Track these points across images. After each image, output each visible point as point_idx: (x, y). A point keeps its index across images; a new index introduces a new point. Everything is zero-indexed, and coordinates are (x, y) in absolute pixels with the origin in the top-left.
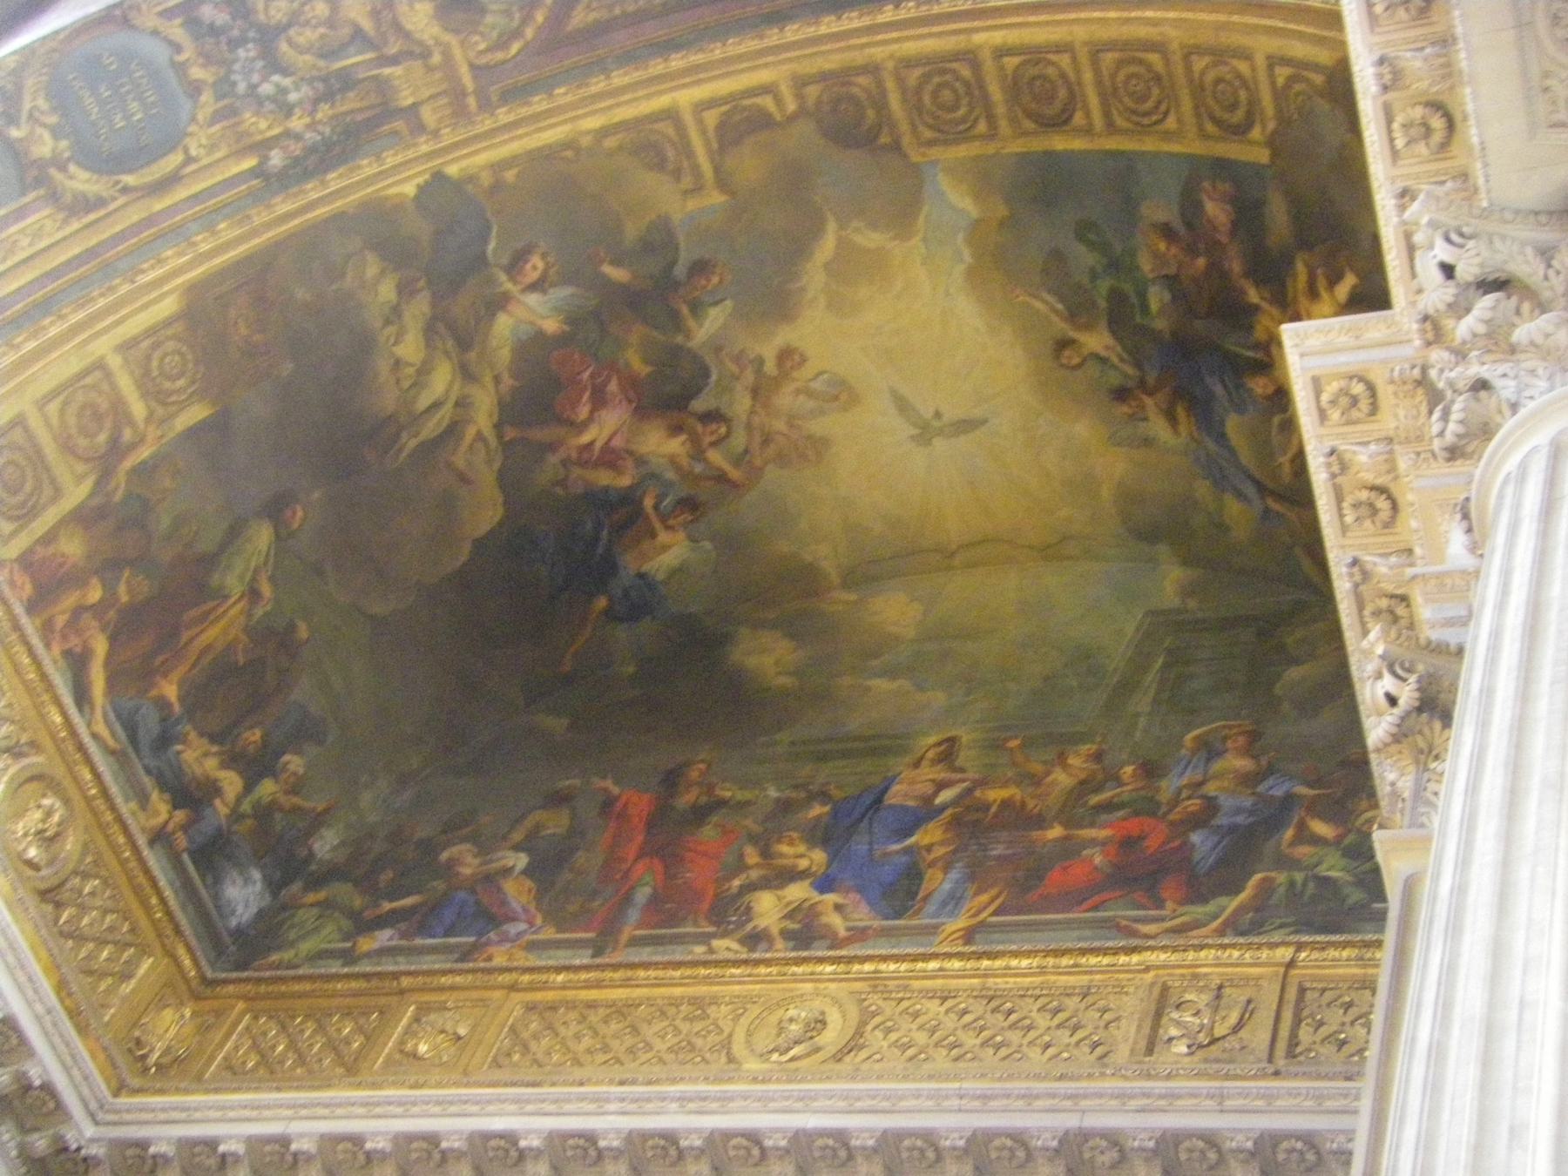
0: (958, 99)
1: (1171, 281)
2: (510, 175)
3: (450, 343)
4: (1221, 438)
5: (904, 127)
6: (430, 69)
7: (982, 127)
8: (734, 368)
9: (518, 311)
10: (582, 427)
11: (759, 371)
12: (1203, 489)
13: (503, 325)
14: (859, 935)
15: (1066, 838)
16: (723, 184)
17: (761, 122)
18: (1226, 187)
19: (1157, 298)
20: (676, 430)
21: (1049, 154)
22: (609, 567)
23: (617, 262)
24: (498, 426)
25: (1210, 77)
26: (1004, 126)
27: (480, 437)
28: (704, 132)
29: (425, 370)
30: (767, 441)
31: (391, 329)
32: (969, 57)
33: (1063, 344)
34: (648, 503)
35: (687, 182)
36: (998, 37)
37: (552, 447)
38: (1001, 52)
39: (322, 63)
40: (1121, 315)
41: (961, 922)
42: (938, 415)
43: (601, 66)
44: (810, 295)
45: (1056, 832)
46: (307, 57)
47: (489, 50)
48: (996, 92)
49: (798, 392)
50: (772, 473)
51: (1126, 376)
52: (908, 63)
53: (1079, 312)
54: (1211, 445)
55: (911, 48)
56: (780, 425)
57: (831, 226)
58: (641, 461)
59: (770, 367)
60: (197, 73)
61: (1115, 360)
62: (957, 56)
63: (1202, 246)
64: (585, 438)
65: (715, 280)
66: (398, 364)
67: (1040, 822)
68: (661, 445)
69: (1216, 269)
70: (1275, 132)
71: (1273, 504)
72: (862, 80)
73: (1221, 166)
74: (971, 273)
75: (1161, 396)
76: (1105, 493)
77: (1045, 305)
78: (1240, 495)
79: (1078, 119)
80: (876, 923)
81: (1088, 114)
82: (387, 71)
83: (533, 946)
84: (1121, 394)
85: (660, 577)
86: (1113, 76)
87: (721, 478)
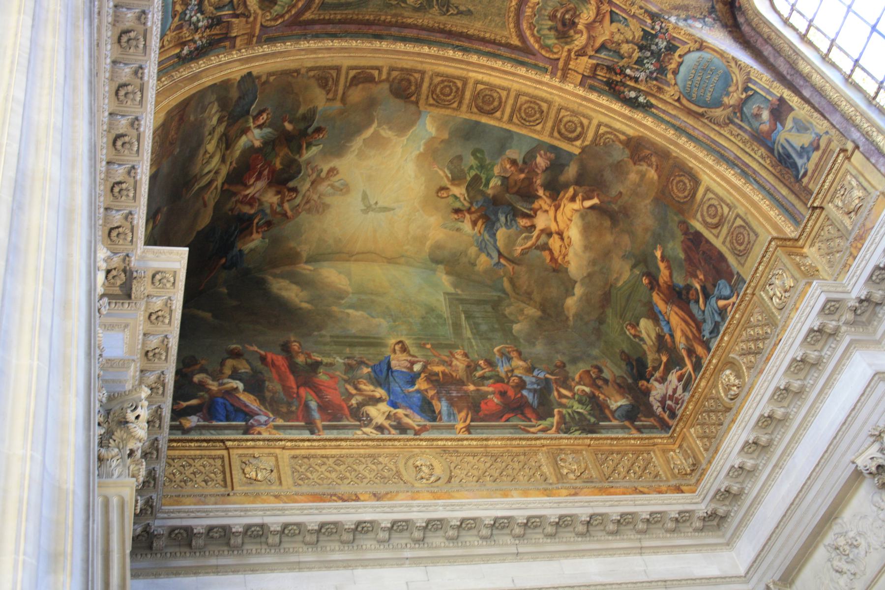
0: (451, 92)
1: (505, 179)
2: (272, 79)
3: (224, 145)
4: (493, 236)
5: (423, 97)
6: (247, 22)
7: (455, 105)
8: (310, 171)
9: (250, 135)
10: (247, 187)
11: (319, 175)
12: (473, 250)
13: (243, 141)
14: (424, 429)
15: (478, 390)
16: (343, 100)
17: (370, 79)
18: (553, 156)
19: (495, 182)
20: (278, 193)
21: (478, 123)
22: (232, 246)
23: (290, 122)
24: (223, 184)
25: (565, 120)
26: (464, 107)
27: (216, 188)
28: (346, 78)
29: (211, 157)
30: (308, 202)
31: (210, 137)
32: (465, 81)
33: (443, 188)
34: (256, 221)
35: (331, 96)
36: (480, 77)
37: (235, 194)
38: (477, 82)
39: (214, 12)
40: (474, 185)
41: (460, 425)
42: (376, 203)
43: (305, 37)
44: (352, 149)
46: (212, 8)
47: (270, 20)
48: (468, 95)
49: (329, 185)
50: (303, 215)
51: (463, 205)
52: (438, 74)
53: (456, 179)
54: (487, 236)
55: (442, 69)
56: (315, 197)
57: (375, 125)
58: (261, 204)
59: (323, 175)
60: (178, 8)
61: (462, 199)
62: (458, 78)
63: (526, 171)
64: (248, 192)
65: (321, 136)
66: (206, 151)
68: (271, 198)
69: (529, 181)
70: (587, 146)
71: (502, 261)
72: (417, 75)
73: (553, 148)
74: (421, 154)
75: (474, 216)
76: (428, 243)
77: (443, 175)
78: (489, 255)
79: (498, 114)
80: (428, 423)
81: (503, 114)
82: (233, 20)
83: (277, 428)
84: (457, 211)
85: (246, 252)
86: (521, 105)
87: (285, 215)
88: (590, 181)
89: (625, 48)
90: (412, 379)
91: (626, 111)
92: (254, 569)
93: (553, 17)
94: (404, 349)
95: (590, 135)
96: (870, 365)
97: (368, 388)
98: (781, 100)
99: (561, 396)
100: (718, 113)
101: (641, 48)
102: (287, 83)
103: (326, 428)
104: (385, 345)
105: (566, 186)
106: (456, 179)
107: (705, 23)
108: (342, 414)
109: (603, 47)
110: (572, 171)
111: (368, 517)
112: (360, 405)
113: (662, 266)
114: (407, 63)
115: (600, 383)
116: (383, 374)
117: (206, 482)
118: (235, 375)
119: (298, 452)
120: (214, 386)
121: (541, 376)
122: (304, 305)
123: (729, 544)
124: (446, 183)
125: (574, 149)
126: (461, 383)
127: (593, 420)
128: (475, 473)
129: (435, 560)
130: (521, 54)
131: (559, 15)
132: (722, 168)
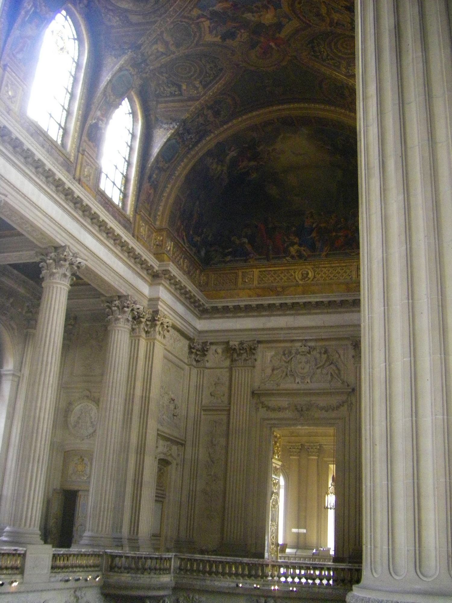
41: (324, 253)
45: (334, 234)
80: (311, 254)
94: (312, 216)
97: (292, 238)
103: (273, 258)
111: (272, 302)
119: (261, 270)
120: (237, 242)
128: (324, 275)
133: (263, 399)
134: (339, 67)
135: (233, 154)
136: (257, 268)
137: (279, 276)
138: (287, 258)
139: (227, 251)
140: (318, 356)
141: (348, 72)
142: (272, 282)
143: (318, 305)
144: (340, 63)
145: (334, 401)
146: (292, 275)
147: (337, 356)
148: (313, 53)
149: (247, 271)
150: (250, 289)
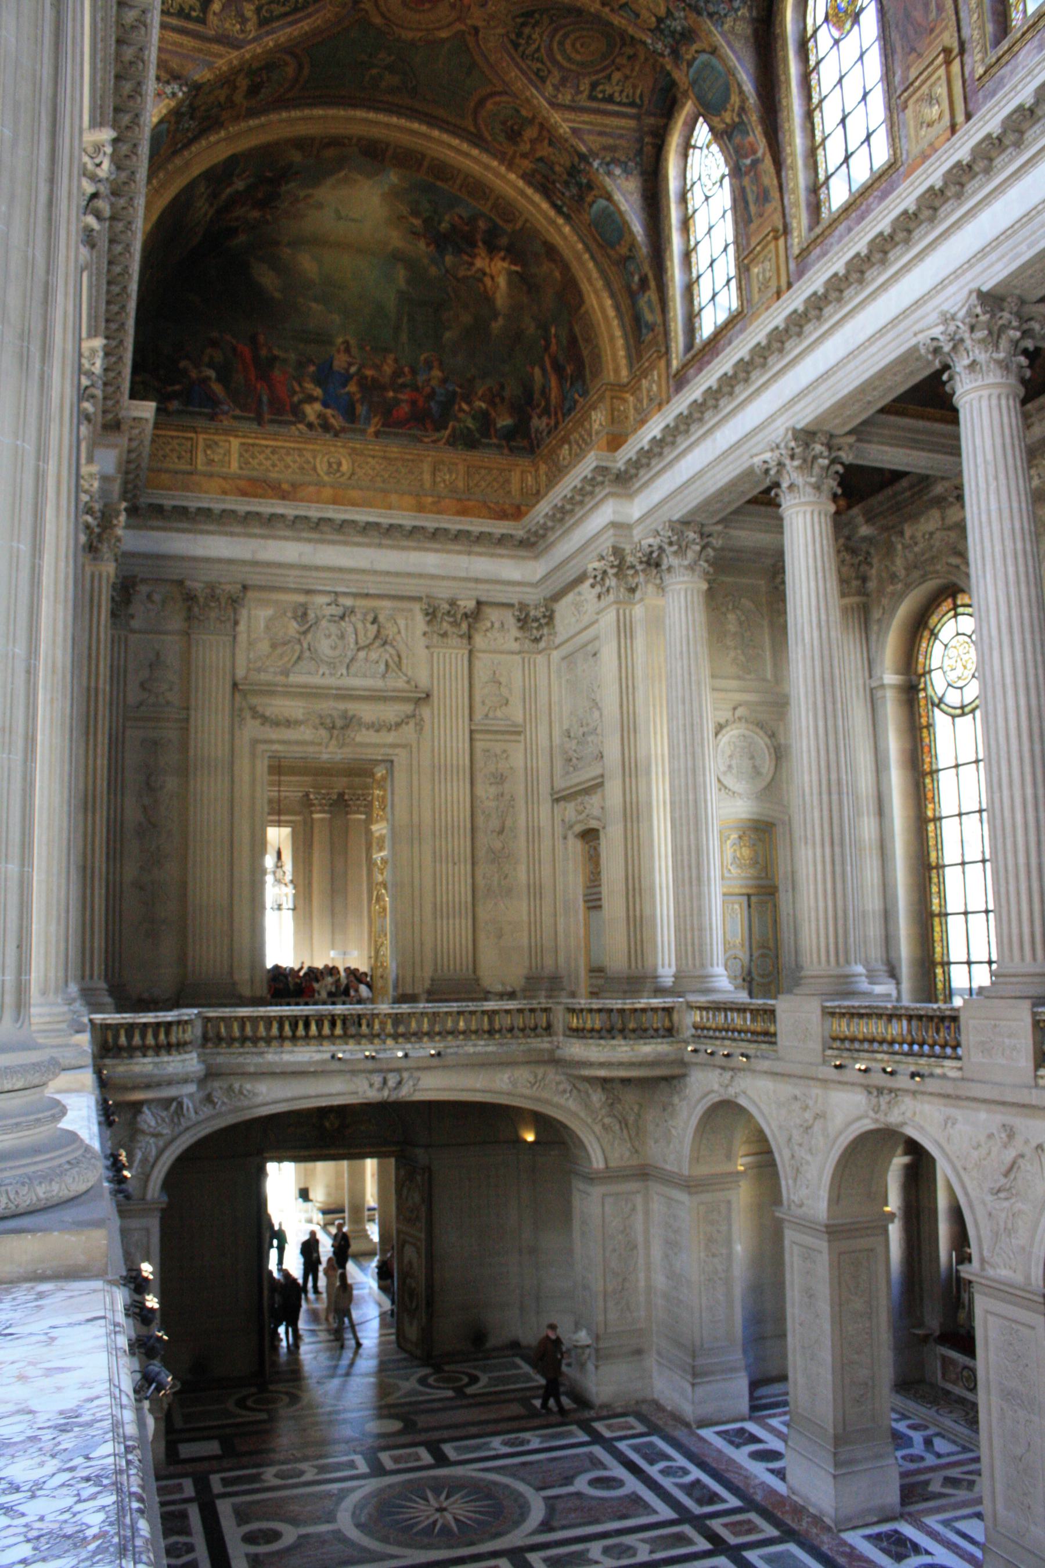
14: (343, 430)
33: (403, 217)
48: (426, 164)
67: (383, 388)
84: (414, 233)
88: (515, 253)
89: (557, 168)
90: (346, 379)
91: (552, 213)
92: (202, 532)
93: (504, 123)
94: (348, 350)
95: (520, 224)
96: (614, 512)
97: (309, 386)
98: (646, 275)
99: (461, 410)
100: (612, 253)
101: (570, 174)
102: (267, 153)
103: (272, 421)
104: (331, 343)
105: (499, 249)
106: (415, 213)
107: (625, 171)
108: (282, 412)
109: (541, 159)
110: (504, 241)
112: (301, 402)
113: (554, 340)
114: (376, 133)
115: (497, 400)
116: (325, 375)
117: (179, 458)
118: (211, 365)
120: (194, 374)
121: (451, 388)
122: (277, 295)
123: (536, 557)
124: (405, 213)
125: (508, 228)
126: (383, 388)
127: (477, 436)
128: (371, 472)
129: (323, 541)
130: (477, 140)
131: (509, 124)
132: (605, 295)
133: (254, 701)
134: (543, 80)
135: (240, 185)
136: (236, 436)
137: (281, 459)
138: (300, 426)
139: (170, 389)
140: (360, 625)
141: (555, 97)
142: (268, 470)
143: (367, 528)
144: (549, 72)
145: (390, 712)
146: (309, 462)
147: (395, 630)
148: (513, 36)
149: (216, 438)
150: (224, 478)
